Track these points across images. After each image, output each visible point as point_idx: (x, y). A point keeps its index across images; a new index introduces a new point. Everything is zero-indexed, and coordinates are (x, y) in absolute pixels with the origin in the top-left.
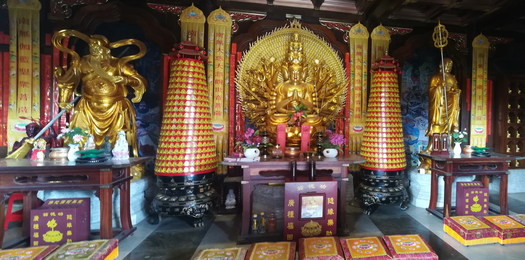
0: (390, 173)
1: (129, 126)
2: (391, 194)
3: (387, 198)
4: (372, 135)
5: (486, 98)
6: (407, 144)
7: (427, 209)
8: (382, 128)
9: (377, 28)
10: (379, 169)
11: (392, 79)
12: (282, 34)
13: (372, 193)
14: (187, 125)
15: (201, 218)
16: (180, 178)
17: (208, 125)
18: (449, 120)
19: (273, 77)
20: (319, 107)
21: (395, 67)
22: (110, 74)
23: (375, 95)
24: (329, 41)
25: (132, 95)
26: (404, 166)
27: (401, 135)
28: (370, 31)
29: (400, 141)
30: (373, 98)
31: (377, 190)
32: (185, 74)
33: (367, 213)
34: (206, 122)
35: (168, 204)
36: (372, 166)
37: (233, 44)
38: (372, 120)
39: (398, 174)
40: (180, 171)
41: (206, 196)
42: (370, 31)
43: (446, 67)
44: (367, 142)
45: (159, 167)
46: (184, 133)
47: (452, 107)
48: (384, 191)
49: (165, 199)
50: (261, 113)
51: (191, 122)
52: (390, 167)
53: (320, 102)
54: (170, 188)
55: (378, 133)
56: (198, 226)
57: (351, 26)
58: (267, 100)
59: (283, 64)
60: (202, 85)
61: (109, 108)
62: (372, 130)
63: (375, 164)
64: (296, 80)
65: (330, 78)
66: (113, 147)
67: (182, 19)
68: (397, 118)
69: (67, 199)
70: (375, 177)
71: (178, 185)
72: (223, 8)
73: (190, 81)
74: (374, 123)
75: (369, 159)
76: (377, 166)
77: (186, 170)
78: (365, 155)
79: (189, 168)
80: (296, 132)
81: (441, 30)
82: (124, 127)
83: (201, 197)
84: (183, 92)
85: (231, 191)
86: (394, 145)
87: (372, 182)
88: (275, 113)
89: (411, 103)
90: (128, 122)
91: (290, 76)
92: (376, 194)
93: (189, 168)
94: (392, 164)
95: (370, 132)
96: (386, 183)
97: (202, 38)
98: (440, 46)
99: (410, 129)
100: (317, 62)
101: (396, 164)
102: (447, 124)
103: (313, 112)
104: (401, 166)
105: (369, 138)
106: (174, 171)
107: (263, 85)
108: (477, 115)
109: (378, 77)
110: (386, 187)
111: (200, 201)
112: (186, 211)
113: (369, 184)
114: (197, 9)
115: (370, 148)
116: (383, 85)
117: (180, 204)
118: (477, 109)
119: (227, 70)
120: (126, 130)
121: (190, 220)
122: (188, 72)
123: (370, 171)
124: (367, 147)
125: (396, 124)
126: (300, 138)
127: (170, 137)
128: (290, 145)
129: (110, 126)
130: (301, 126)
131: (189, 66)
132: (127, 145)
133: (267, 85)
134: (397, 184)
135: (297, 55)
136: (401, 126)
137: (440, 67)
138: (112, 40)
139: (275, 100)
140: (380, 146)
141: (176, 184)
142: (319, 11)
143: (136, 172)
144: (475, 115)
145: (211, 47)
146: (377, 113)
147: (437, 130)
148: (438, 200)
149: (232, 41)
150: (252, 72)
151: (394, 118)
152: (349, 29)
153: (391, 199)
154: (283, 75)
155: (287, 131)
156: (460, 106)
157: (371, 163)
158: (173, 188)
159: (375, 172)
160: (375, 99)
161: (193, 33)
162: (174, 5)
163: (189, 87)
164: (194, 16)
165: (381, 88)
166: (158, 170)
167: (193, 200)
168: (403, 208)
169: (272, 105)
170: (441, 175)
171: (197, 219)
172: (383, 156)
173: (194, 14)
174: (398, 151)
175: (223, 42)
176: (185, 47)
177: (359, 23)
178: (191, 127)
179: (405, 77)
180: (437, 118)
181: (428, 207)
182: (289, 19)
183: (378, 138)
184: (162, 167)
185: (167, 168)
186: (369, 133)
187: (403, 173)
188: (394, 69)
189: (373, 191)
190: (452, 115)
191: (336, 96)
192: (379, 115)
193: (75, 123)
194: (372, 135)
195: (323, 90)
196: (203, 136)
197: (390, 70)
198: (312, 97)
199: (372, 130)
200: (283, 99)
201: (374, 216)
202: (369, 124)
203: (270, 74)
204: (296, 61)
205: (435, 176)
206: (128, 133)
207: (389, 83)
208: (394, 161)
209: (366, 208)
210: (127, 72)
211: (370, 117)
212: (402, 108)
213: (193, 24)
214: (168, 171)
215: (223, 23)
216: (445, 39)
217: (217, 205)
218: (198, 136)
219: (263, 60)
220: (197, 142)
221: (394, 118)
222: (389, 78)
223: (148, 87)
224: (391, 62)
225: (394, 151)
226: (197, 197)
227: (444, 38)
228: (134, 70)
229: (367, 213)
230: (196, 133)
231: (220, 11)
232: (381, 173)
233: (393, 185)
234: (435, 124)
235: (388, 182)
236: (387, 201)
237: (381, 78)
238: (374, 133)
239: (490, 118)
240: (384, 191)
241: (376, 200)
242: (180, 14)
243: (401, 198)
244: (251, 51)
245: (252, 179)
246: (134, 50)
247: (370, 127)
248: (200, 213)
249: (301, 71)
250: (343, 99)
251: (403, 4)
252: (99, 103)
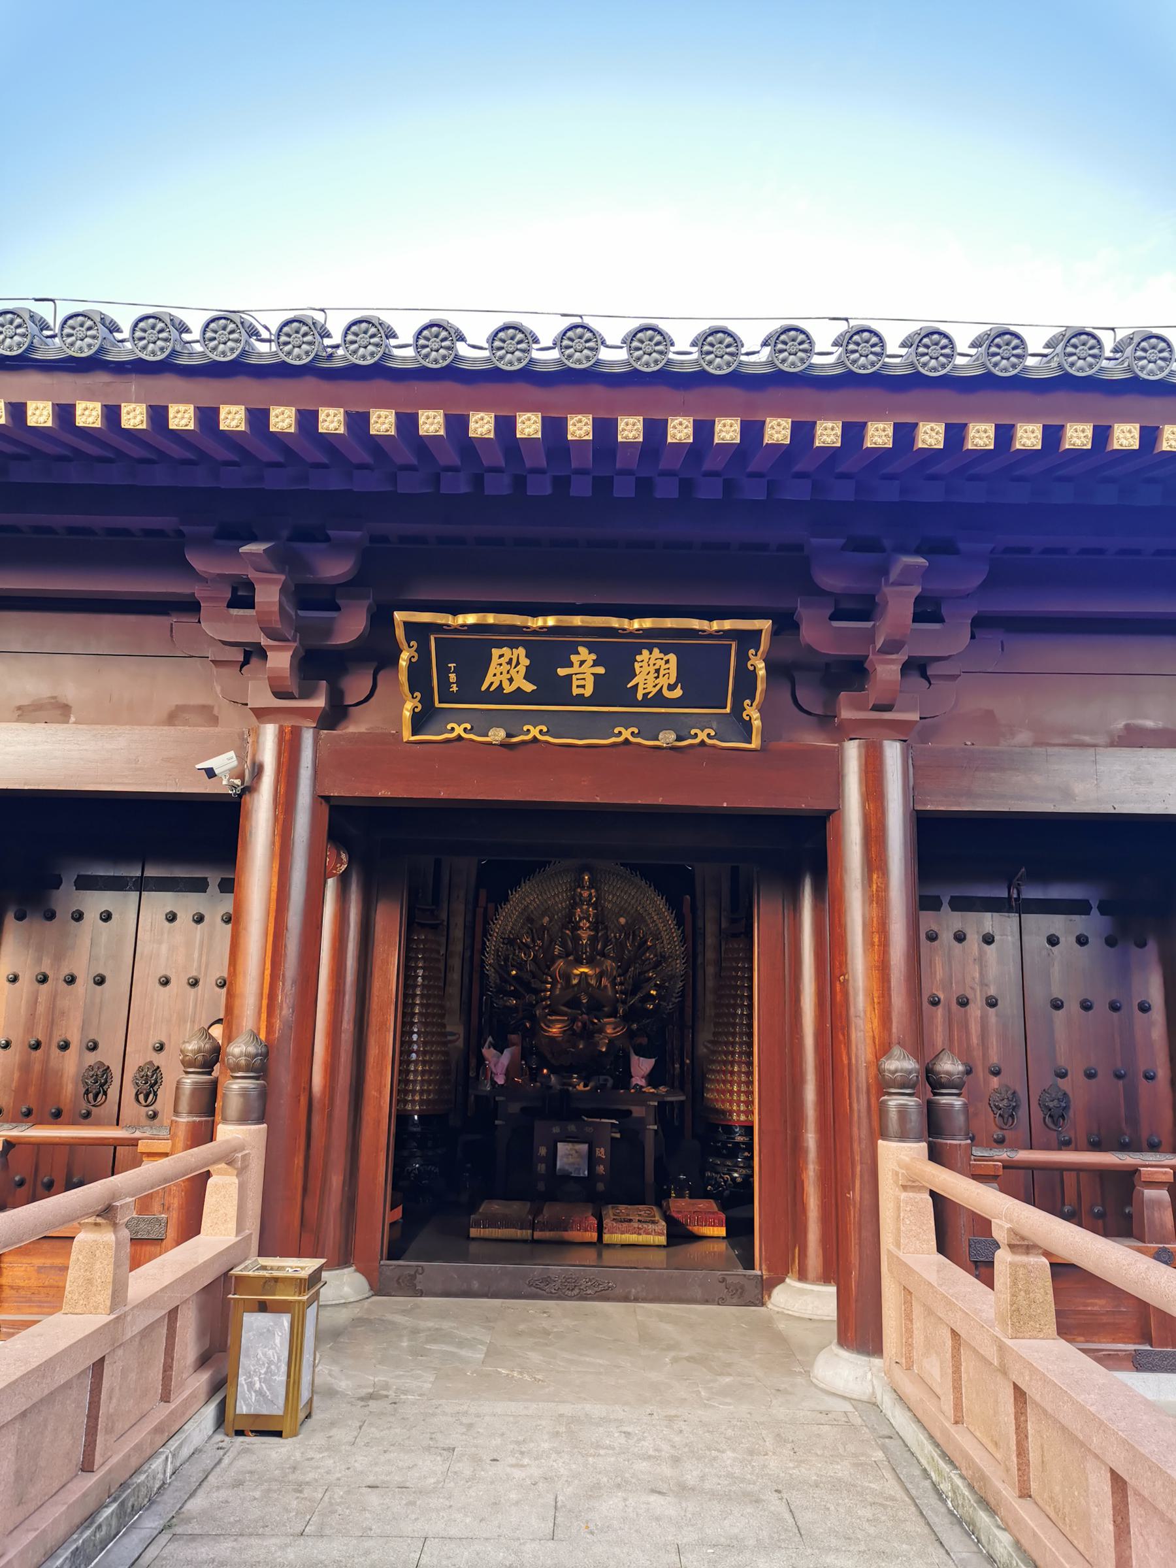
13: (720, 1169)
19: (548, 949)
58: (536, 992)
59: (564, 927)
63: (723, 1112)
65: (649, 948)
70: (724, 1137)
100: (622, 921)
103: (613, 1014)
135: (587, 910)
150: (510, 942)
169: (545, 999)
191: (652, 984)
198: (614, 984)
200: (562, 989)
204: (585, 924)
219: (530, 920)
241: (725, 1182)
249: (593, 940)
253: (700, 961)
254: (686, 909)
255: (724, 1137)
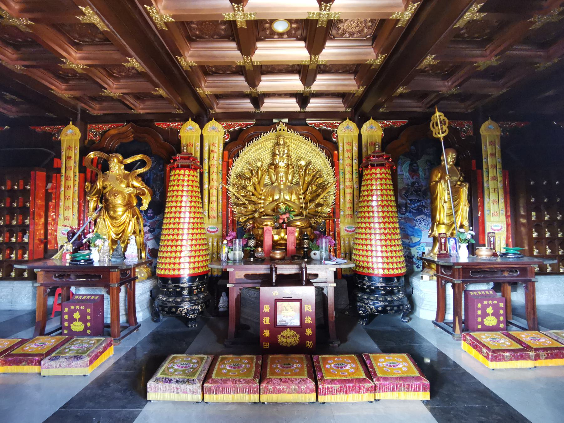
0: (387, 279)
1: (138, 232)
2: (389, 304)
3: (384, 307)
4: (364, 236)
5: (503, 190)
6: (407, 247)
7: (433, 322)
8: (375, 229)
9: (368, 122)
10: (373, 274)
11: (384, 175)
12: (269, 139)
13: (367, 301)
14: (183, 229)
15: (195, 319)
16: (177, 280)
17: (200, 229)
18: (456, 218)
20: (306, 209)
21: (387, 161)
22: (123, 186)
23: (365, 193)
24: (315, 140)
25: (140, 204)
26: (403, 271)
27: (399, 237)
28: (360, 127)
29: (397, 242)
30: (364, 196)
31: (372, 298)
32: (181, 183)
33: (363, 324)
34: (199, 226)
35: (166, 304)
36: (366, 271)
37: (225, 152)
38: (363, 220)
39: (396, 280)
40: (176, 273)
41: (199, 297)
42: (360, 127)
43: (448, 159)
44: (359, 244)
45: (159, 269)
46: (180, 237)
47: (458, 204)
48: (381, 299)
49: (164, 299)
50: (251, 216)
51: (186, 226)
52: (386, 272)
53: (306, 203)
54: (168, 288)
55: (370, 234)
56: (192, 326)
57: (339, 124)
58: (254, 203)
59: (269, 168)
60: (196, 192)
61: (123, 214)
62: (364, 231)
63: (368, 268)
64: (282, 183)
66: (125, 250)
67: (181, 134)
68: (392, 217)
69: (91, 295)
70: (369, 283)
71: (175, 286)
72: (216, 120)
73: (185, 188)
74: (365, 223)
75: (361, 263)
76: (371, 271)
77: (181, 272)
78: (357, 258)
79: (185, 272)
80: (282, 234)
81: (440, 119)
82: (134, 233)
83: (195, 298)
84: (179, 199)
85: (223, 294)
86: (389, 247)
87: (367, 289)
88: (264, 216)
89: (410, 200)
90: (137, 227)
91: (277, 179)
92: (371, 302)
93: (185, 272)
94: (388, 269)
95: (362, 234)
96: (382, 290)
97: (198, 149)
98: (439, 136)
99: (411, 229)
101: (393, 269)
102: (453, 223)
103: (301, 214)
104: (400, 271)
105: (360, 240)
106: (172, 272)
107: (250, 189)
108: (492, 211)
109: (369, 174)
110: (383, 295)
111: (193, 303)
112: (181, 312)
113: (363, 290)
114: (194, 123)
115: (363, 250)
116: (374, 182)
117: (176, 304)
118: (491, 204)
119: (220, 176)
120: (135, 235)
121: (185, 320)
122: (183, 180)
123: (364, 277)
124: (359, 250)
125: (391, 224)
126: (286, 240)
127: (168, 241)
128: (277, 247)
129: (123, 231)
130: (286, 228)
131: (184, 175)
132: (136, 248)
133: (255, 188)
134: (396, 291)
136: (397, 226)
137: (442, 158)
138: (126, 157)
139: (263, 203)
140: (374, 248)
141: (173, 285)
142: (305, 112)
143: (143, 273)
144: (489, 211)
145: (206, 156)
146: (368, 212)
147: (442, 229)
148: (447, 312)
149: (224, 150)
151: (388, 217)
152: (337, 127)
153: (388, 308)
154: (271, 178)
155: (273, 233)
156: (470, 201)
157: (364, 268)
158: (170, 288)
159: (370, 278)
160: (366, 198)
161: (189, 145)
162: (175, 121)
163: (185, 194)
164: (191, 129)
165: (372, 185)
166: (158, 272)
167: (187, 301)
168: (405, 319)
170: (448, 282)
171: (191, 320)
172: (379, 259)
173: (191, 127)
174: (395, 255)
175: (217, 151)
176: (182, 158)
177: (348, 120)
178: (186, 231)
179: (401, 173)
180: (442, 215)
181: (434, 318)
182: (276, 123)
183: (371, 240)
184: (162, 269)
185: (165, 269)
186: (360, 235)
187: (402, 279)
188: (385, 164)
189: (369, 299)
190: (459, 212)
192: (371, 214)
193: (98, 230)
194: (364, 236)
195: (309, 191)
196: (196, 240)
197: (382, 166)
198: (299, 199)
199: (364, 231)
201: (370, 327)
202: (360, 224)
203: (258, 178)
204: (282, 164)
205: (442, 283)
206: (137, 237)
207: (381, 179)
208: (391, 266)
209: (362, 317)
210: (136, 183)
211: (361, 217)
212: (399, 206)
213: (190, 136)
214: (167, 273)
215: (216, 133)
216: (445, 128)
217: (210, 305)
218: (192, 240)
220: (191, 245)
221: (388, 217)
222: (381, 174)
223: (153, 195)
224: (382, 156)
225: (390, 254)
226: (191, 298)
227: (443, 126)
228: (142, 182)
229: (363, 324)
230: (190, 237)
231: (213, 123)
232: (377, 279)
233: (391, 293)
234: (439, 224)
235: (385, 289)
236: (384, 311)
237: (371, 174)
238: (366, 234)
239: (509, 214)
240: (381, 299)
241: (371, 309)
242: (180, 128)
243: (401, 307)
244: (241, 157)
245: (239, 282)
246: (143, 164)
247: (362, 228)
248: (194, 314)
250: (331, 200)
251: (394, 95)
252: (115, 212)
253: (341, 187)
254: (335, 159)
255: (369, 283)
